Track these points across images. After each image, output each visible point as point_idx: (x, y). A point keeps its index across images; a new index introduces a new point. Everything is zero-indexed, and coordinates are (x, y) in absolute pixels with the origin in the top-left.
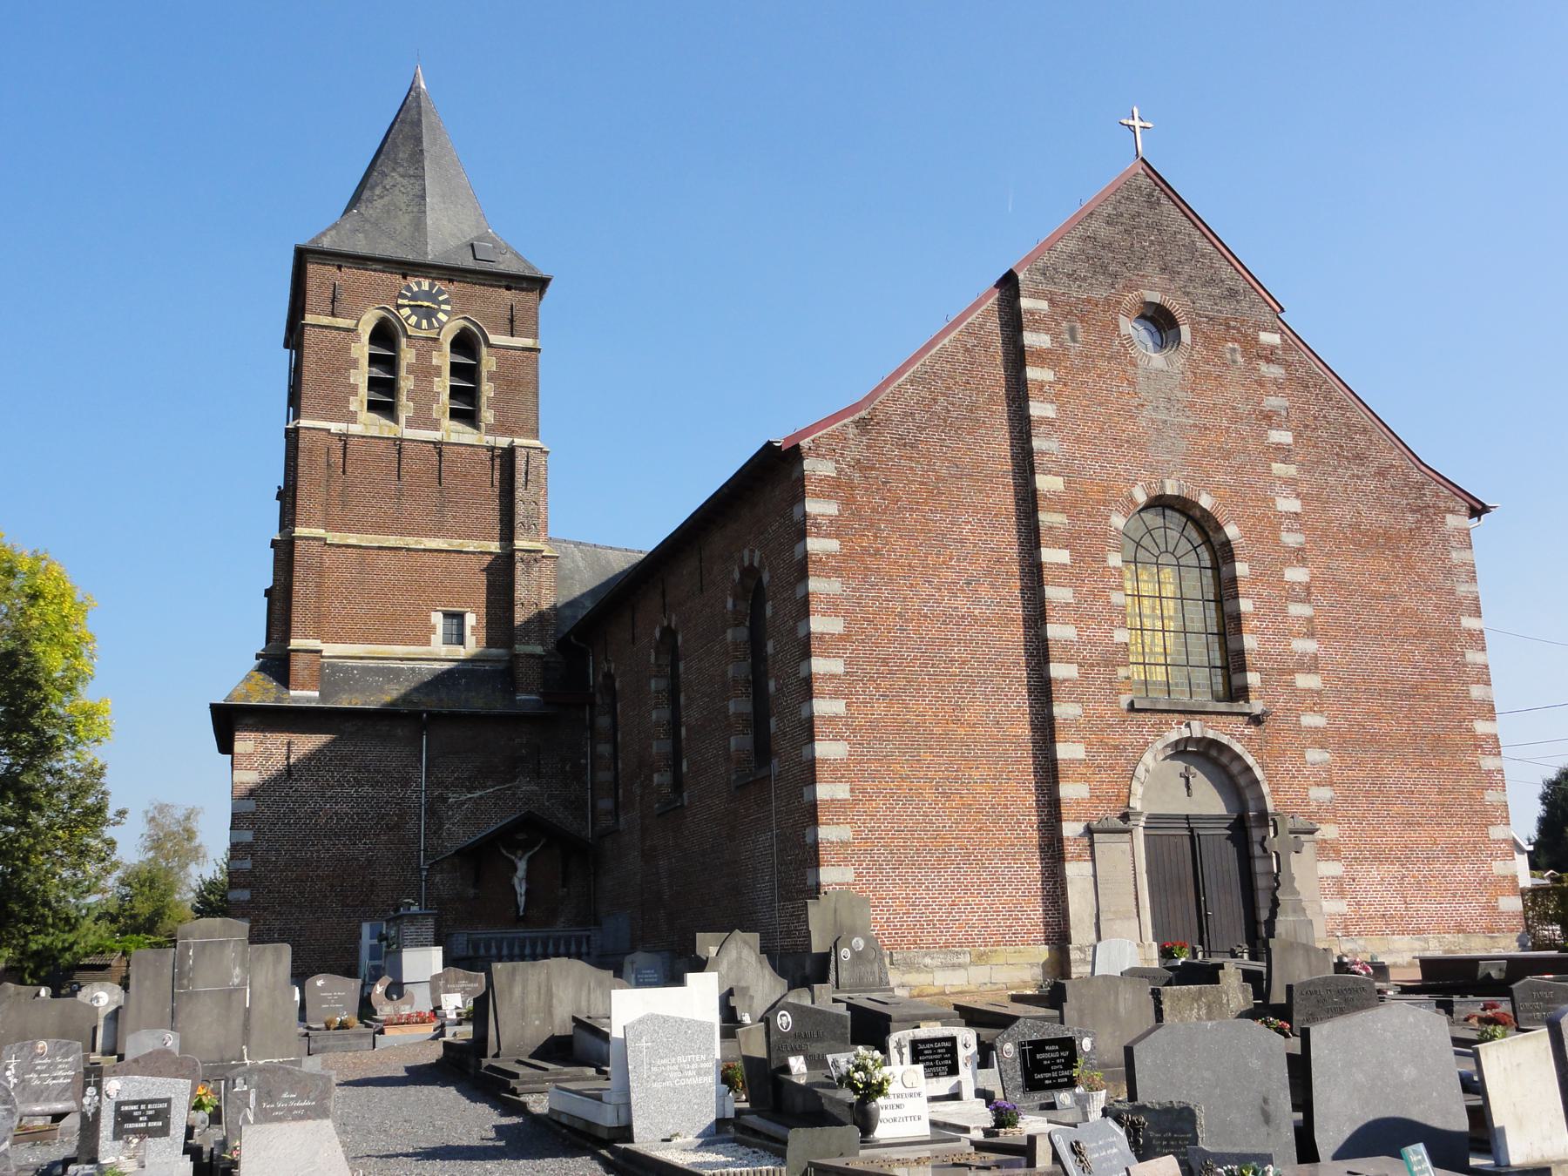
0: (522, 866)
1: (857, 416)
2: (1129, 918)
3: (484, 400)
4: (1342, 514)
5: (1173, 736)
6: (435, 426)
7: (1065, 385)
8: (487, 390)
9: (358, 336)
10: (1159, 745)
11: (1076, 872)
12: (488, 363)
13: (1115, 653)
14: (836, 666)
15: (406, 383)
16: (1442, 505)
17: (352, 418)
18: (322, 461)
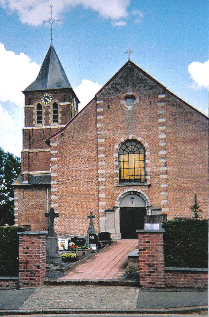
1: (61, 133)
3: (59, 118)
4: (181, 136)
7: (106, 118)
8: (60, 115)
9: (34, 108)
12: (60, 110)
13: (114, 175)
14: (56, 182)
15: (44, 116)
18: (28, 136)
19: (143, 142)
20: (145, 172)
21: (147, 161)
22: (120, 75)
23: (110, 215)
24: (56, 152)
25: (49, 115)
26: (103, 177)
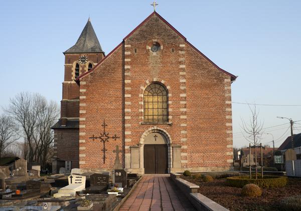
2: (137, 164)
4: (198, 81)
5: (150, 129)
10: (147, 131)
11: (127, 155)
16: (224, 77)
19: (166, 85)
20: (168, 112)
21: (170, 102)
22: (145, 24)
23: (135, 151)
24: (85, 90)
26: (129, 116)
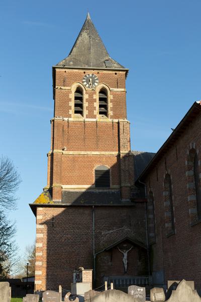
0: (126, 255)
6: (95, 117)
8: (110, 105)
9: (71, 91)
12: (110, 97)
15: (85, 104)
17: (70, 116)
18: (61, 129)
25: (95, 103)
